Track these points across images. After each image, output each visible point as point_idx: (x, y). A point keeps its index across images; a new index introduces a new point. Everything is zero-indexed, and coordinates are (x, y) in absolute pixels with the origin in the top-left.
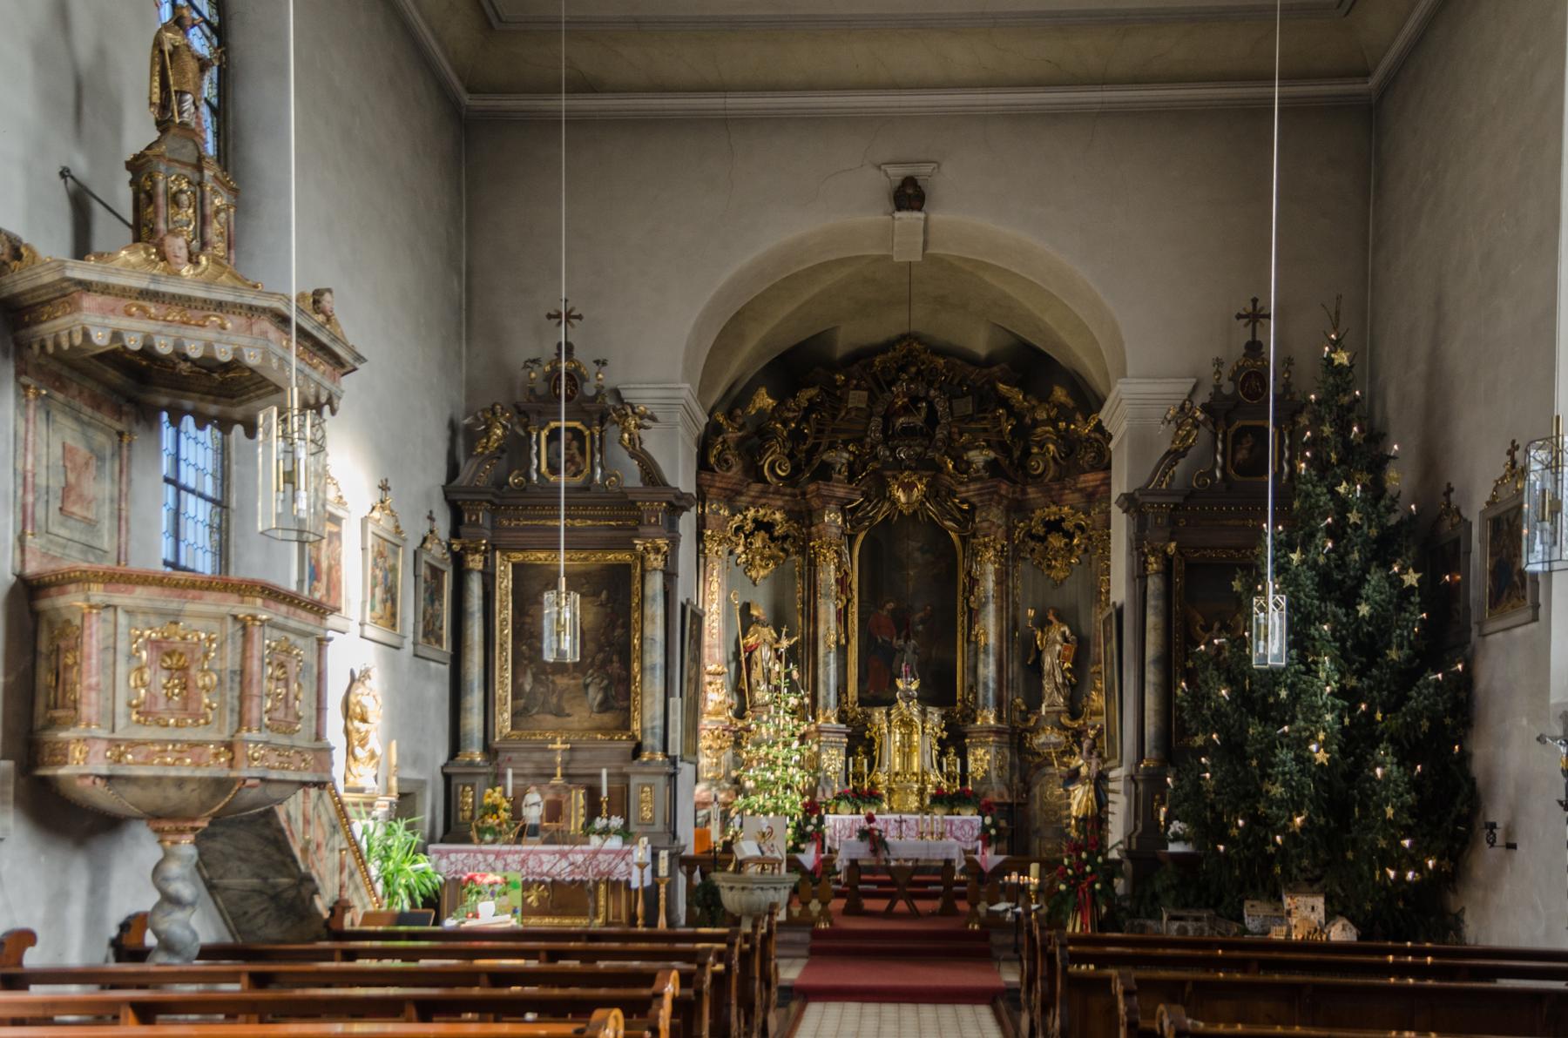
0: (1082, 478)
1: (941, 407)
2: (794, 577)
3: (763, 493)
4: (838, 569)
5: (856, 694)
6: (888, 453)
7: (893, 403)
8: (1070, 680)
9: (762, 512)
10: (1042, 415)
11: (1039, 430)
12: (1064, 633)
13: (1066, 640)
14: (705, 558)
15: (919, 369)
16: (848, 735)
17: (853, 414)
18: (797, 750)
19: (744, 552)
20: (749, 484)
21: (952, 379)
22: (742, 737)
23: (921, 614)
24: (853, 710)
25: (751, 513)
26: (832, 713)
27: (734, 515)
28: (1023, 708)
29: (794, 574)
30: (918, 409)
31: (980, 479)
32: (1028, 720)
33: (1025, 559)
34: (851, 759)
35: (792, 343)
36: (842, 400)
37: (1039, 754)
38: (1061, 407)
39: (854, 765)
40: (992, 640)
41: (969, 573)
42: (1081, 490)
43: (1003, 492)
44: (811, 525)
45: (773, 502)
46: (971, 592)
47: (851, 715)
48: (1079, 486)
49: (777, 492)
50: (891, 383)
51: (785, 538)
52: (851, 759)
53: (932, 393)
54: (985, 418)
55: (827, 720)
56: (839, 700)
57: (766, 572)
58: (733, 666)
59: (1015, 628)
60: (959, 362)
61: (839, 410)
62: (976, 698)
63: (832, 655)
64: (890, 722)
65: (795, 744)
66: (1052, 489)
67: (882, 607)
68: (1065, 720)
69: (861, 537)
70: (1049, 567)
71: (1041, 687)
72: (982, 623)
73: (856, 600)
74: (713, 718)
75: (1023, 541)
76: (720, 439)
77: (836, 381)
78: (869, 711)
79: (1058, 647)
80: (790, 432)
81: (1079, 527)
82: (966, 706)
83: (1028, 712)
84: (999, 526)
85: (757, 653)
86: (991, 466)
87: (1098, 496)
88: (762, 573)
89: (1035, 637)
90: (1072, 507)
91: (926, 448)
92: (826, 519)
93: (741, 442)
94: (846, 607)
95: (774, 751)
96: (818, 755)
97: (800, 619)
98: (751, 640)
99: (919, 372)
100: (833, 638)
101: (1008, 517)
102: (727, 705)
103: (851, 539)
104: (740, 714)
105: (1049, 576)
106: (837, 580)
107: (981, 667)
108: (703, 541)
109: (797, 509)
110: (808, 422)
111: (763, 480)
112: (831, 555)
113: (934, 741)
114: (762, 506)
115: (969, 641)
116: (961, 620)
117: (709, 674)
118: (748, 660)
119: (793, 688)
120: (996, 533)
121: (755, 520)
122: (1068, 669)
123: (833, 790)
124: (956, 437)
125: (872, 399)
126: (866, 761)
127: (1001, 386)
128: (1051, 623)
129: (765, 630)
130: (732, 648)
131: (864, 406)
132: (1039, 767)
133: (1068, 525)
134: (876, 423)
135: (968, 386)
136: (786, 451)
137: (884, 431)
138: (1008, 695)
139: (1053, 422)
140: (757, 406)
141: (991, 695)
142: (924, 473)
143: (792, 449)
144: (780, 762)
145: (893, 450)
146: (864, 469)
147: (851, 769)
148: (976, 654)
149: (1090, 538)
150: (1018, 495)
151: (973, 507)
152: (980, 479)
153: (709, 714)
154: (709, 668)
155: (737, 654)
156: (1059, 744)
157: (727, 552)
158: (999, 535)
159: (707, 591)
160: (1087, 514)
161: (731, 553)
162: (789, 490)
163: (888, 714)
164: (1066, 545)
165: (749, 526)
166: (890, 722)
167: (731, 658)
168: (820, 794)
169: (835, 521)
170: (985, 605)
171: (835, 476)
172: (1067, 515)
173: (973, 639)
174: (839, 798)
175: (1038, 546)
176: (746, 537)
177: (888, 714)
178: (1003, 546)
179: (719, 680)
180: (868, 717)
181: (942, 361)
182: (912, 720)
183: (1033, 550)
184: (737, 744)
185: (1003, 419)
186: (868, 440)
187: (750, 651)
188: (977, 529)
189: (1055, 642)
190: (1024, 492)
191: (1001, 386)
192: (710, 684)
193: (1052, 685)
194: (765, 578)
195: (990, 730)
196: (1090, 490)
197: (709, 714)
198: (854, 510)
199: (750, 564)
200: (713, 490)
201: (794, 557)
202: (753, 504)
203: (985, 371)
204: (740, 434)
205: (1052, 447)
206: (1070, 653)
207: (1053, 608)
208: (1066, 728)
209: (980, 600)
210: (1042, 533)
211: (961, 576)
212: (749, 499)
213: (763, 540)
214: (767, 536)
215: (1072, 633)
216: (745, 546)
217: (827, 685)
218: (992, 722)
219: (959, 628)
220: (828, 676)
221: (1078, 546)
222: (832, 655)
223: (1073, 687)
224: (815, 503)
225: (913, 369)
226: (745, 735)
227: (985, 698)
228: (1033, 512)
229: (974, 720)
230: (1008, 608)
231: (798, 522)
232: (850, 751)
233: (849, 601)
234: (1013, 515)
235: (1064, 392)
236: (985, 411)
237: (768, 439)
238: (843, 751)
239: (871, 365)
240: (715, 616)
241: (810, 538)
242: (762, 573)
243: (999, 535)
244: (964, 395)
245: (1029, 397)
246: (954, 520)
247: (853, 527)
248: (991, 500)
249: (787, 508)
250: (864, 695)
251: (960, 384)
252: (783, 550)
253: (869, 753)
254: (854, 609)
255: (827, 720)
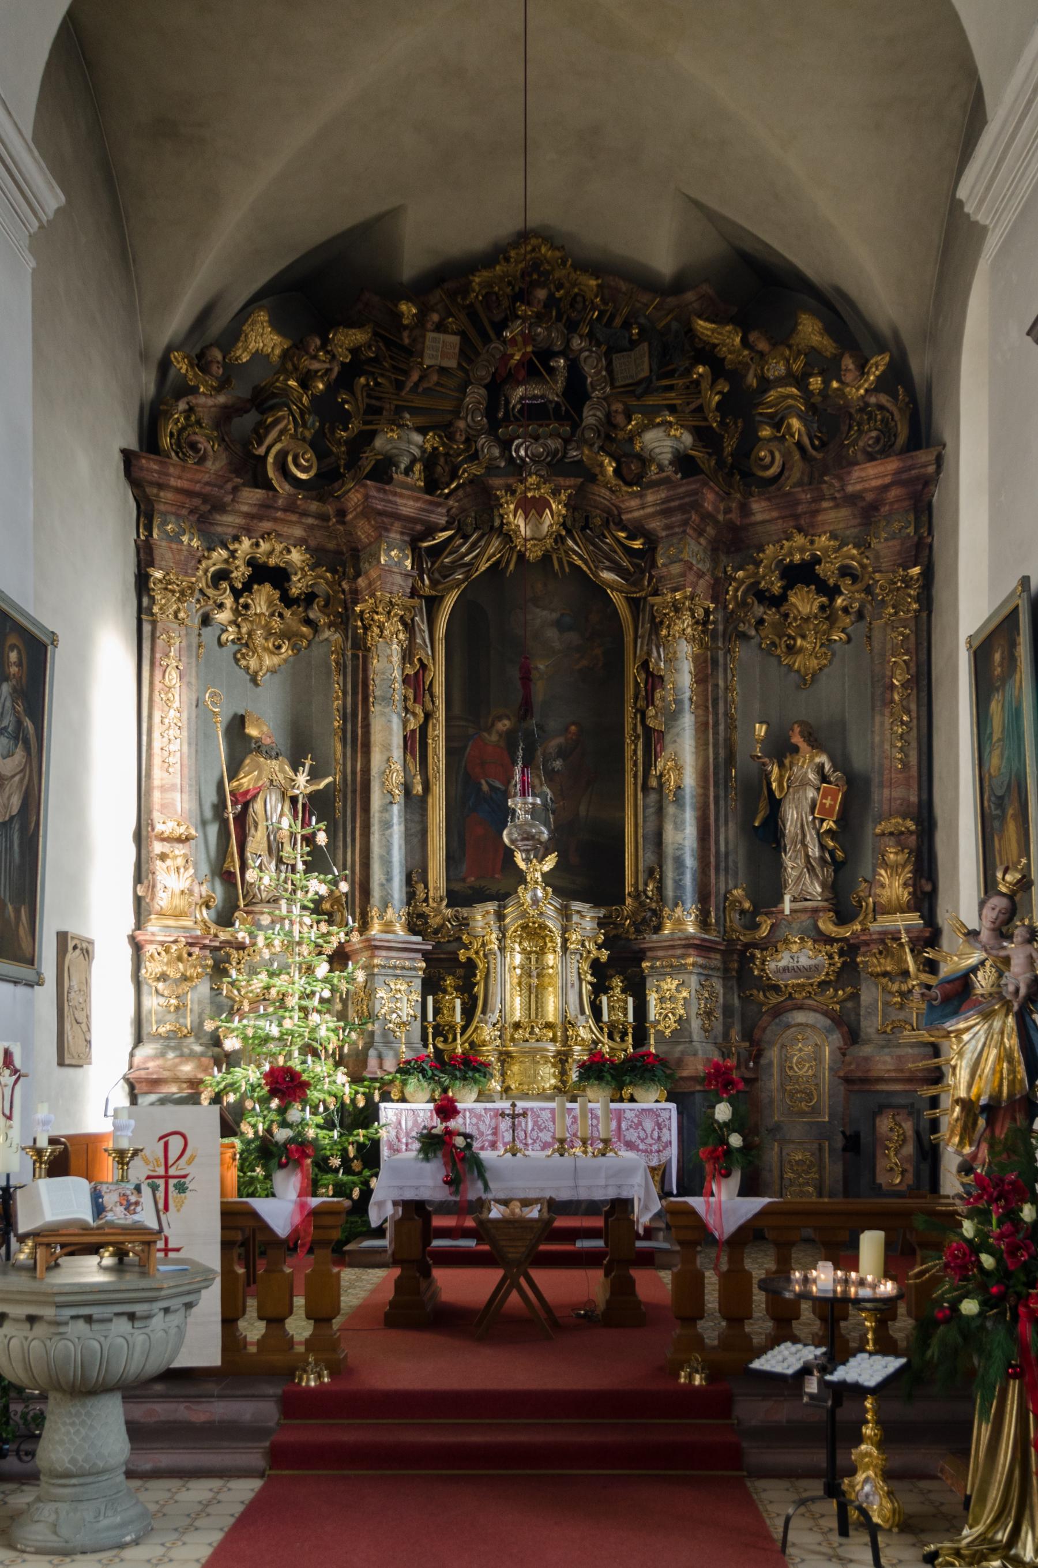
0: (856, 473)
1: (592, 369)
2: (329, 674)
3: (264, 511)
4: (407, 655)
5: (443, 885)
6: (496, 452)
7: (506, 357)
8: (832, 853)
9: (264, 546)
10: (776, 368)
11: (772, 395)
12: (820, 768)
13: (824, 779)
14: (154, 623)
15: (551, 296)
16: (426, 956)
17: (435, 378)
18: (326, 980)
19: (234, 623)
20: (235, 490)
21: (612, 317)
22: (227, 959)
23: (560, 740)
24: (438, 911)
25: (246, 545)
26: (396, 914)
27: (211, 549)
28: (747, 905)
29: (329, 666)
30: (551, 371)
31: (666, 482)
32: (756, 926)
33: (744, 637)
34: (430, 999)
35: (324, 238)
36: (412, 352)
37: (776, 988)
38: (813, 354)
39: (437, 1011)
40: (689, 780)
41: (645, 665)
42: (852, 499)
43: (708, 506)
44: (358, 574)
45: (285, 530)
46: (650, 700)
47: (434, 922)
48: (850, 489)
49: (291, 507)
50: (501, 326)
51: (309, 598)
52: (430, 999)
53: (576, 343)
54: (670, 388)
55: (388, 928)
56: (411, 897)
57: (276, 660)
58: (213, 830)
59: (730, 759)
60: (624, 286)
61: (406, 373)
62: (660, 889)
63: (395, 808)
64: (503, 930)
65: (322, 969)
66: (797, 503)
67: (489, 729)
68: (827, 925)
69: (450, 601)
70: (791, 649)
71: (780, 866)
72: (670, 749)
73: (441, 714)
74: (171, 922)
75: (743, 604)
76: (182, 406)
77: (400, 315)
78: (464, 912)
79: (811, 793)
80: (314, 399)
81: (845, 571)
82: (642, 904)
83: (756, 912)
84: (700, 575)
85: (258, 806)
86: (684, 463)
87: (885, 509)
88: (268, 661)
89: (767, 776)
90: (833, 536)
91: (567, 441)
92: (383, 560)
93: (225, 416)
94: (424, 728)
95: (280, 983)
96: (368, 988)
97: (339, 747)
98: (246, 781)
99: (551, 302)
100: (397, 778)
101: (715, 561)
102: (196, 898)
103: (433, 604)
104: (225, 919)
105: (790, 667)
106: (406, 680)
107: (669, 830)
108: (148, 590)
109: (331, 546)
110: (351, 390)
111: (268, 486)
112: (393, 626)
113: (585, 966)
114: (266, 536)
115: (645, 788)
116: (633, 750)
117: (163, 839)
118: (241, 819)
119: (316, 863)
120: (694, 586)
121: (251, 562)
122: (829, 831)
123: (397, 1055)
124: (620, 419)
125: (468, 353)
126: (458, 1002)
127: (703, 326)
128: (796, 749)
129: (274, 764)
130: (211, 797)
131: (452, 363)
132: (778, 1012)
133: (827, 570)
134: (476, 395)
135: (641, 328)
136: (308, 434)
137: (490, 413)
138: (719, 883)
139: (800, 381)
140: (253, 346)
141: (688, 880)
142: (561, 481)
143: (320, 433)
144: (292, 1002)
145: (505, 445)
146: (454, 476)
147: (430, 1018)
148: (660, 811)
149: (868, 590)
150: (734, 516)
151: (652, 543)
152: (666, 482)
153: (161, 914)
154: (159, 828)
155: (219, 808)
156: (817, 968)
157: (197, 620)
158: (699, 591)
159: (158, 686)
160: (862, 544)
161: (206, 620)
162: (314, 506)
163: (500, 917)
164: (822, 608)
165: (241, 572)
166: (503, 930)
167: (209, 814)
168: (372, 1062)
169: (399, 564)
170: (673, 717)
171: (398, 477)
172: (825, 550)
173: (654, 783)
174: (405, 1070)
175: (771, 615)
176: (237, 594)
177: (500, 917)
178: (707, 612)
179: (180, 850)
180: (464, 924)
181: (593, 283)
182: (543, 927)
183: (761, 622)
184: (219, 971)
185: (705, 385)
186: (461, 424)
187: (246, 802)
188: (660, 579)
189: (805, 783)
190: (745, 510)
191: (703, 326)
192: (163, 857)
193: (801, 862)
194: (273, 671)
195: (690, 945)
196: (869, 497)
197: (161, 914)
198: (436, 552)
199: (244, 644)
200: (167, 495)
201: (327, 634)
202: (249, 532)
203: (672, 301)
204: (221, 399)
205: (796, 423)
206: (834, 802)
207: (801, 723)
208: (829, 940)
209: (666, 708)
210: (777, 588)
211: (632, 670)
212: (239, 521)
213: (270, 603)
214: (277, 594)
215: (835, 768)
216: (236, 612)
217: (387, 862)
218: (691, 929)
219: (629, 765)
220: (388, 847)
221: (846, 610)
222: (395, 808)
223: (838, 866)
224: (364, 531)
225: (541, 294)
226: (235, 954)
227: (679, 885)
228: (761, 549)
229: (658, 929)
230: (716, 724)
231: (334, 571)
232: (431, 986)
233: (428, 716)
234: (723, 558)
235: (818, 325)
236: (670, 375)
237: (272, 408)
238: (417, 983)
239: (466, 290)
240: (173, 732)
241: (355, 596)
242: (268, 661)
243: (699, 591)
244: (633, 344)
245: (752, 337)
246: (617, 569)
247: (434, 583)
248: (685, 523)
249: (313, 543)
250: (457, 887)
251: (627, 325)
252: (308, 622)
253: (466, 988)
254: (438, 731)
255: (388, 928)
